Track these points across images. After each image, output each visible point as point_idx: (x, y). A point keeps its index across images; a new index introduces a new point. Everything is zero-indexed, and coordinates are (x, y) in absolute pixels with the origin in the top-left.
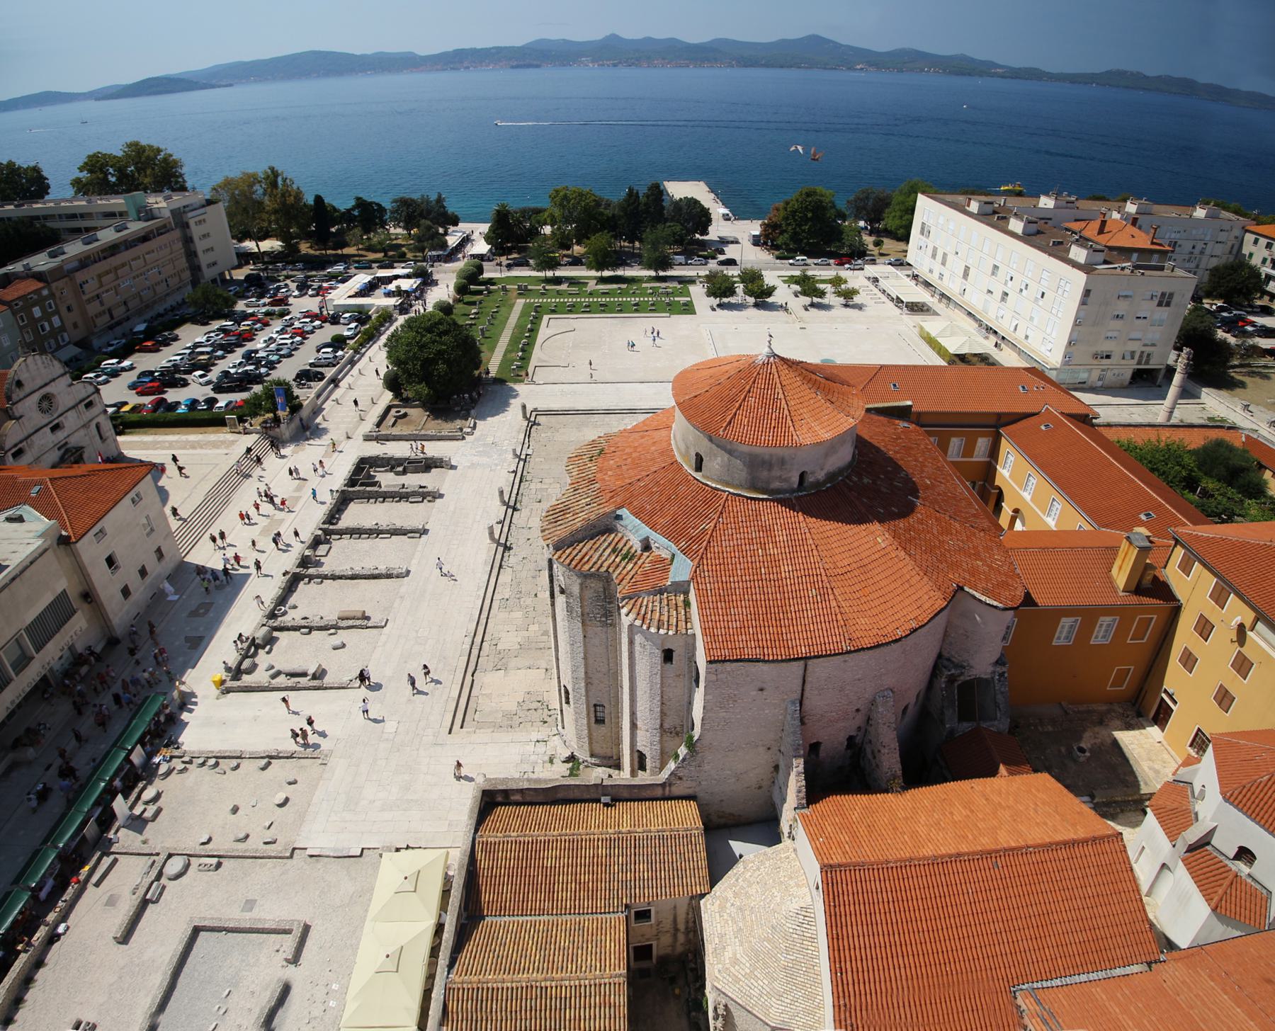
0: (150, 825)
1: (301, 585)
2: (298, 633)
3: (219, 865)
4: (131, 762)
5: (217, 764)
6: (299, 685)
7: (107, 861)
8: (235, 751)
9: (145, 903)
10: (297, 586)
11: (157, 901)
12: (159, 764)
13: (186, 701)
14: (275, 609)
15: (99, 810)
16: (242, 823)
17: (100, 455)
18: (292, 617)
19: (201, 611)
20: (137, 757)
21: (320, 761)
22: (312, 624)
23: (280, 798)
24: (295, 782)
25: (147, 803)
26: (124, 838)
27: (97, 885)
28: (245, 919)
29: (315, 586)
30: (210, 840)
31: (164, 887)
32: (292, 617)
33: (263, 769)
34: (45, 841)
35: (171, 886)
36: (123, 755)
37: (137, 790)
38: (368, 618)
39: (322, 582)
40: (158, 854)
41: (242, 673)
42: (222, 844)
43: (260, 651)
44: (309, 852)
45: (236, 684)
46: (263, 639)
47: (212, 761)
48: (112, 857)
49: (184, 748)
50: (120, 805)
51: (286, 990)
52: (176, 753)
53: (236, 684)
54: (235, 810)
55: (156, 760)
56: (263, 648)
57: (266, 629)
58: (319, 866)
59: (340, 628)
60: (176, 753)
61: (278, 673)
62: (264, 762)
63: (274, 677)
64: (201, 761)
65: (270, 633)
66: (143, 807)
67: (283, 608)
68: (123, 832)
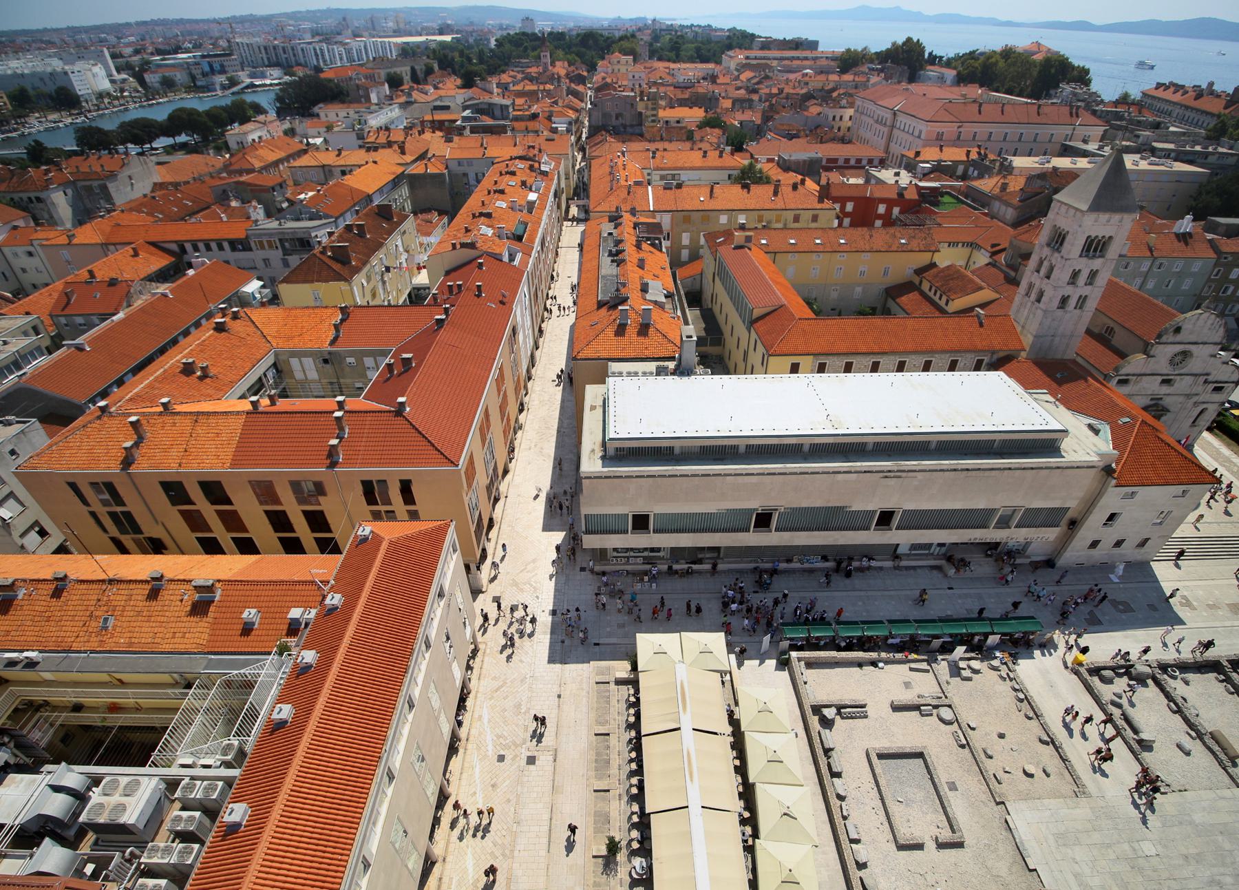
0: (958, 679)
1: (1212, 675)
2: (1166, 701)
3: (962, 746)
4: (986, 638)
5: (1021, 701)
6: (1123, 732)
7: (924, 666)
8: (1039, 709)
9: (917, 708)
10: (1208, 672)
11: (923, 715)
12: (996, 658)
13: (1047, 646)
14: (1171, 666)
15: (950, 639)
16: (996, 747)
17: (1187, 438)
18: (1176, 686)
19: (1121, 607)
20: (993, 640)
21: (1076, 790)
22: (1184, 710)
23: (1031, 769)
24: (1048, 775)
25: (969, 667)
26: (942, 667)
27: (911, 669)
28: (944, 790)
29: (1223, 689)
30: (973, 729)
31: (931, 715)
32: (1176, 686)
33: (1041, 741)
34: (916, 621)
35: (935, 718)
36: (989, 630)
37: (973, 655)
38: (1235, 765)
39: (1232, 693)
40: (946, 697)
41: (1098, 675)
42: (976, 739)
43: (1125, 679)
44: (1008, 818)
45: (1086, 675)
46: (1139, 674)
47: (1021, 696)
48: (929, 668)
49: (1017, 667)
50: (960, 651)
51: (919, 847)
52: (1010, 664)
53: (1086, 675)
54: (1001, 736)
55: (998, 654)
56: (1131, 679)
57: (1148, 670)
58: (1004, 833)
59: (1202, 740)
60: (1010, 664)
61: (1119, 706)
62: (1046, 738)
63: (1113, 703)
64: (1017, 687)
65: (1148, 676)
66: (965, 666)
67: (1178, 673)
68: (944, 663)
